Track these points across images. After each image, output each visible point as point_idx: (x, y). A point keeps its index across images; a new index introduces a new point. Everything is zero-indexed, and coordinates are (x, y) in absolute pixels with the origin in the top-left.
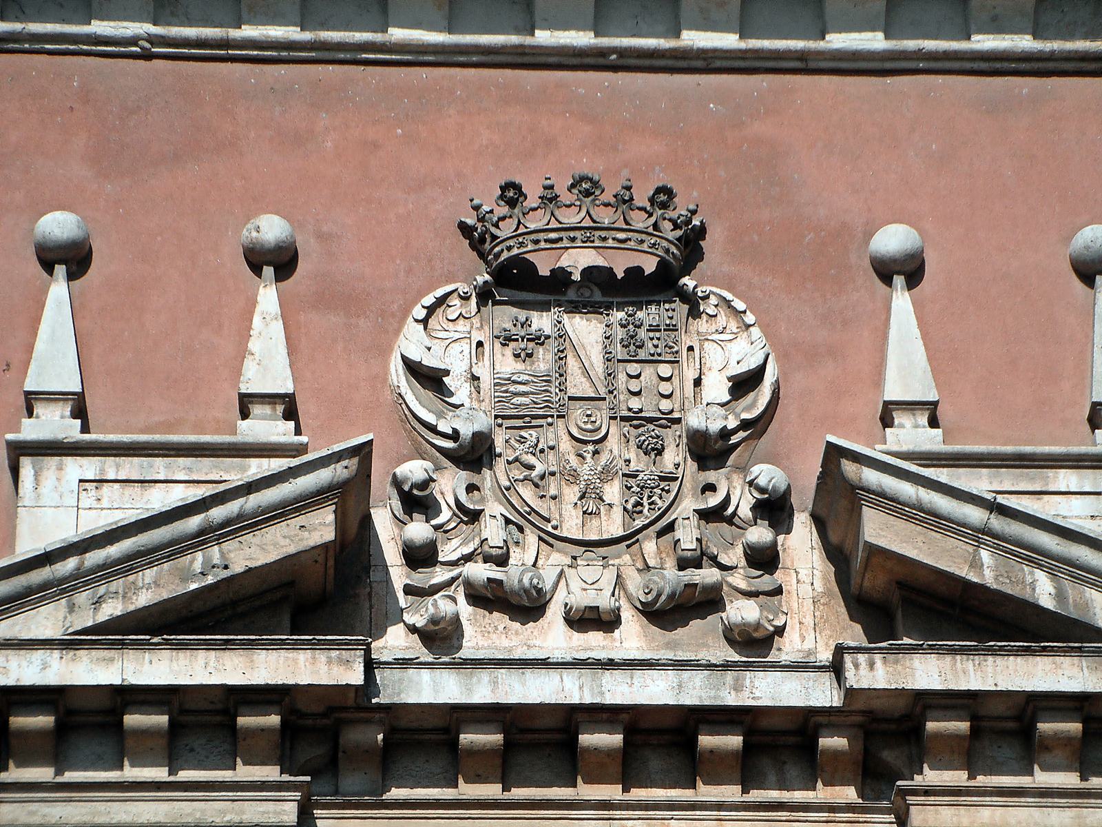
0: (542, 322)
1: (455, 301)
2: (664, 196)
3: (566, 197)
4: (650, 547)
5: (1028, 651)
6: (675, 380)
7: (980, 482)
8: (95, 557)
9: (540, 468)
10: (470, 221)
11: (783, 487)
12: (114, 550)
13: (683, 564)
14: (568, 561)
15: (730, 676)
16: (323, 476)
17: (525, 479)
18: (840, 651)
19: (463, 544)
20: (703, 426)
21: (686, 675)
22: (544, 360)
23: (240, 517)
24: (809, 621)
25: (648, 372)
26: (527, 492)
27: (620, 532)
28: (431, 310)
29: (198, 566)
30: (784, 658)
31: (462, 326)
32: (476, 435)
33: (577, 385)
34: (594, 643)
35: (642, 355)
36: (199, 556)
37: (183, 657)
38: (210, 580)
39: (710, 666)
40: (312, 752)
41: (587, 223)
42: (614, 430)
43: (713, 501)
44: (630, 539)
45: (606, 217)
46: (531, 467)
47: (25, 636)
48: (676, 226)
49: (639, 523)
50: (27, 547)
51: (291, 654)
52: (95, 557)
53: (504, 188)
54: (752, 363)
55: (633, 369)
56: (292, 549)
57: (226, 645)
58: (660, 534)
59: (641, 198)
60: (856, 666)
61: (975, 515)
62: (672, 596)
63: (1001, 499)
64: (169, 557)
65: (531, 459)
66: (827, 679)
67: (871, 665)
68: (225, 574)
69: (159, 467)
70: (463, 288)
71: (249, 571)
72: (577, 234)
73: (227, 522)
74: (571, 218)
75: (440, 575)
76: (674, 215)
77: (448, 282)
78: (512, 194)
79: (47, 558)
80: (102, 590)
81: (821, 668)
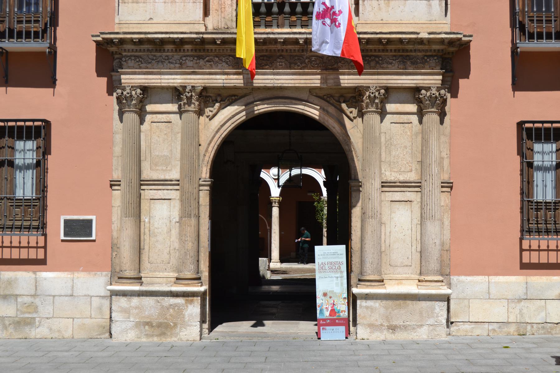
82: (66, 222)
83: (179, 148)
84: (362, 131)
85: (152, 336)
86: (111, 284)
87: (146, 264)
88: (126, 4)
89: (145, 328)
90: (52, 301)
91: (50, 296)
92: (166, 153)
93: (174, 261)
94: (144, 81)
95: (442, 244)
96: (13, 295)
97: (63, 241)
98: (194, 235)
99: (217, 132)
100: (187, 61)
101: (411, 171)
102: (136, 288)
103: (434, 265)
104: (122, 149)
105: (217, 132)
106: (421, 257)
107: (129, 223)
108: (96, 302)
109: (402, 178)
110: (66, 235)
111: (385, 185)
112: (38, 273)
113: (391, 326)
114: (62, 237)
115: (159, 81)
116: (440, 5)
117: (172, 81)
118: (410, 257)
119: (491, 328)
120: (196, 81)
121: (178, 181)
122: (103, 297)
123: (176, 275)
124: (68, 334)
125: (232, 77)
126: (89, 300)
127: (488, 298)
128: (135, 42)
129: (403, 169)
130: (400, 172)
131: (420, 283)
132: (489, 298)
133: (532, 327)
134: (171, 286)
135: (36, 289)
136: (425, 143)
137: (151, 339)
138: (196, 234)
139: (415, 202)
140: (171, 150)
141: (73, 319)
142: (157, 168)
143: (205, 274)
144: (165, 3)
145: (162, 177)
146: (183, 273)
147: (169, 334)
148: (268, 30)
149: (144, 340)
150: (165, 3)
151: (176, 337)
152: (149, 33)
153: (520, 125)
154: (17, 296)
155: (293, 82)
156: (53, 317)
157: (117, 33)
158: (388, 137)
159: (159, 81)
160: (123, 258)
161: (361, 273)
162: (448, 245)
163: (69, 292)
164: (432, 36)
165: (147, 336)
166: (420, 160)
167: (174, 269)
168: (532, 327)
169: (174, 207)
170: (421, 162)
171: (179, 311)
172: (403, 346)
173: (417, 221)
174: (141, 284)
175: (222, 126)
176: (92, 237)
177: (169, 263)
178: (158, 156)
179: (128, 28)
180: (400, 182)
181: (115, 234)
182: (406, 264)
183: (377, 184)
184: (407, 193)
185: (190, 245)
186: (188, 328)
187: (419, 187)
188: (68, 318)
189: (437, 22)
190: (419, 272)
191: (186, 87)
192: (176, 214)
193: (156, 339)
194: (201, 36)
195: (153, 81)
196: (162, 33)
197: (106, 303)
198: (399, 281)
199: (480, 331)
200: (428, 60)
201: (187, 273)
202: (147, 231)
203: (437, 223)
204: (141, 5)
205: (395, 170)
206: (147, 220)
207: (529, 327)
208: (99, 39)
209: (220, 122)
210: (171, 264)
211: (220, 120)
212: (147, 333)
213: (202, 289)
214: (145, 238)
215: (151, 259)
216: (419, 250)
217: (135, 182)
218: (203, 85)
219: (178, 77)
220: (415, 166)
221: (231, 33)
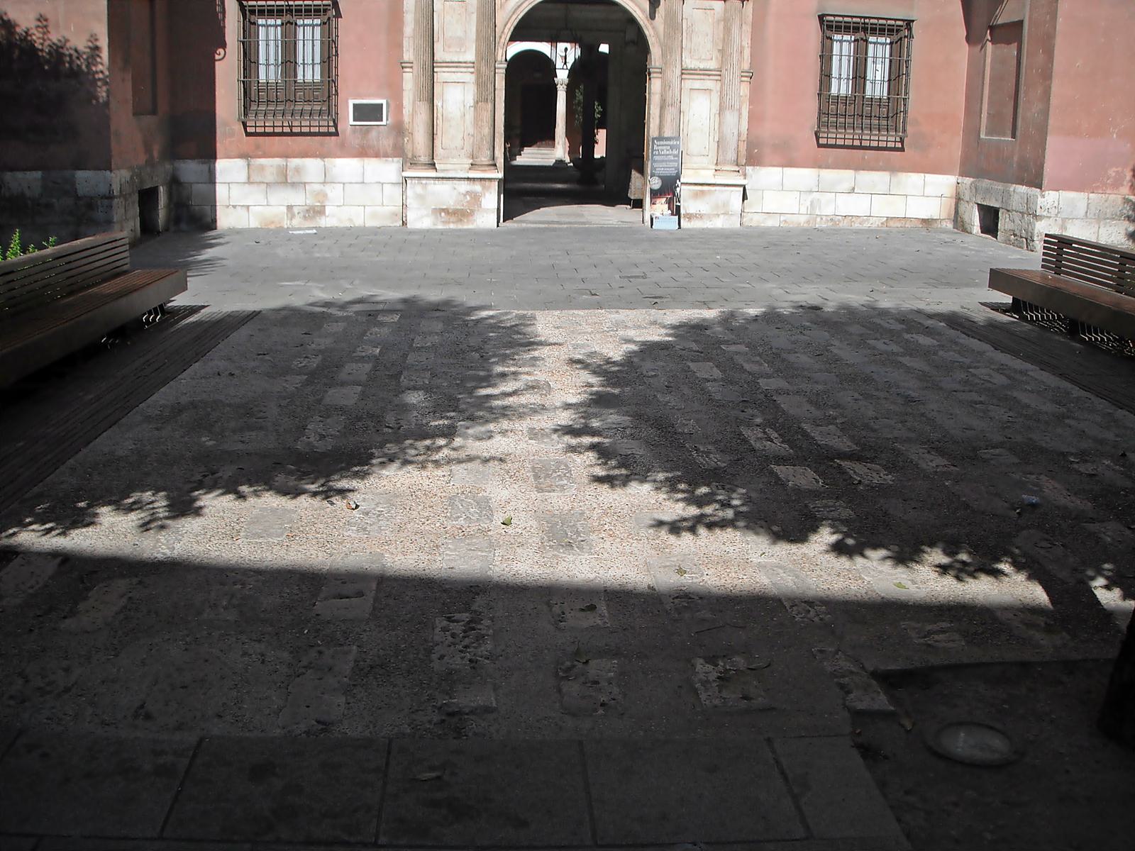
82: (355, 106)
83: (474, 29)
84: (663, 16)
85: (449, 222)
87: (439, 151)
89: (440, 214)
92: (460, 33)
93: (468, 148)
95: (739, 135)
96: (302, 183)
98: (491, 122)
99: (514, 13)
103: (731, 155)
104: (414, 30)
105: (514, 13)
106: (718, 146)
107: (423, 109)
111: (684, 71)
113: (688, 214)
114: (352, 122)
118: (707, 147)
119: (782, 218)
121: (474, 63)
123: (471, 161)
129: (703, 57)
130: (700, 59)
133: (822, 219)
134: (468, 172)
136: (727, 30)
138: (493, 118)
141: (364, 206)
142: (451, 50)
146: (479, 160)
147: (465, 221)
149: (440, 226)
151: (473, 224)
154: (305, 183)
158: (689, 24)
160: (417, 144)
162: (746, 136)
163: (360, 180)
166: (721, 48)
167: (469, 155)
168: (822, 219)
170: (722, 52)
171: (476, 198)
173: (715, 110)
175: (519, 7)
177: (463, 149)
180: (701, 70)
181: (406, 119)
183: (678, 72)
184: (708, 81)
185: (487, 130)
192: (470, 100)
197: (398, 190)
199: (771, 223)
201: (483, 159)
203: (736, 114)
205: (695, 57)
206: (440, 105)
207: (818, 219)
210: (465, 149)
212: (443, 220)
214: (439, 122)
216: (717, 139)
217: (429, 63)
220: (715, 54)
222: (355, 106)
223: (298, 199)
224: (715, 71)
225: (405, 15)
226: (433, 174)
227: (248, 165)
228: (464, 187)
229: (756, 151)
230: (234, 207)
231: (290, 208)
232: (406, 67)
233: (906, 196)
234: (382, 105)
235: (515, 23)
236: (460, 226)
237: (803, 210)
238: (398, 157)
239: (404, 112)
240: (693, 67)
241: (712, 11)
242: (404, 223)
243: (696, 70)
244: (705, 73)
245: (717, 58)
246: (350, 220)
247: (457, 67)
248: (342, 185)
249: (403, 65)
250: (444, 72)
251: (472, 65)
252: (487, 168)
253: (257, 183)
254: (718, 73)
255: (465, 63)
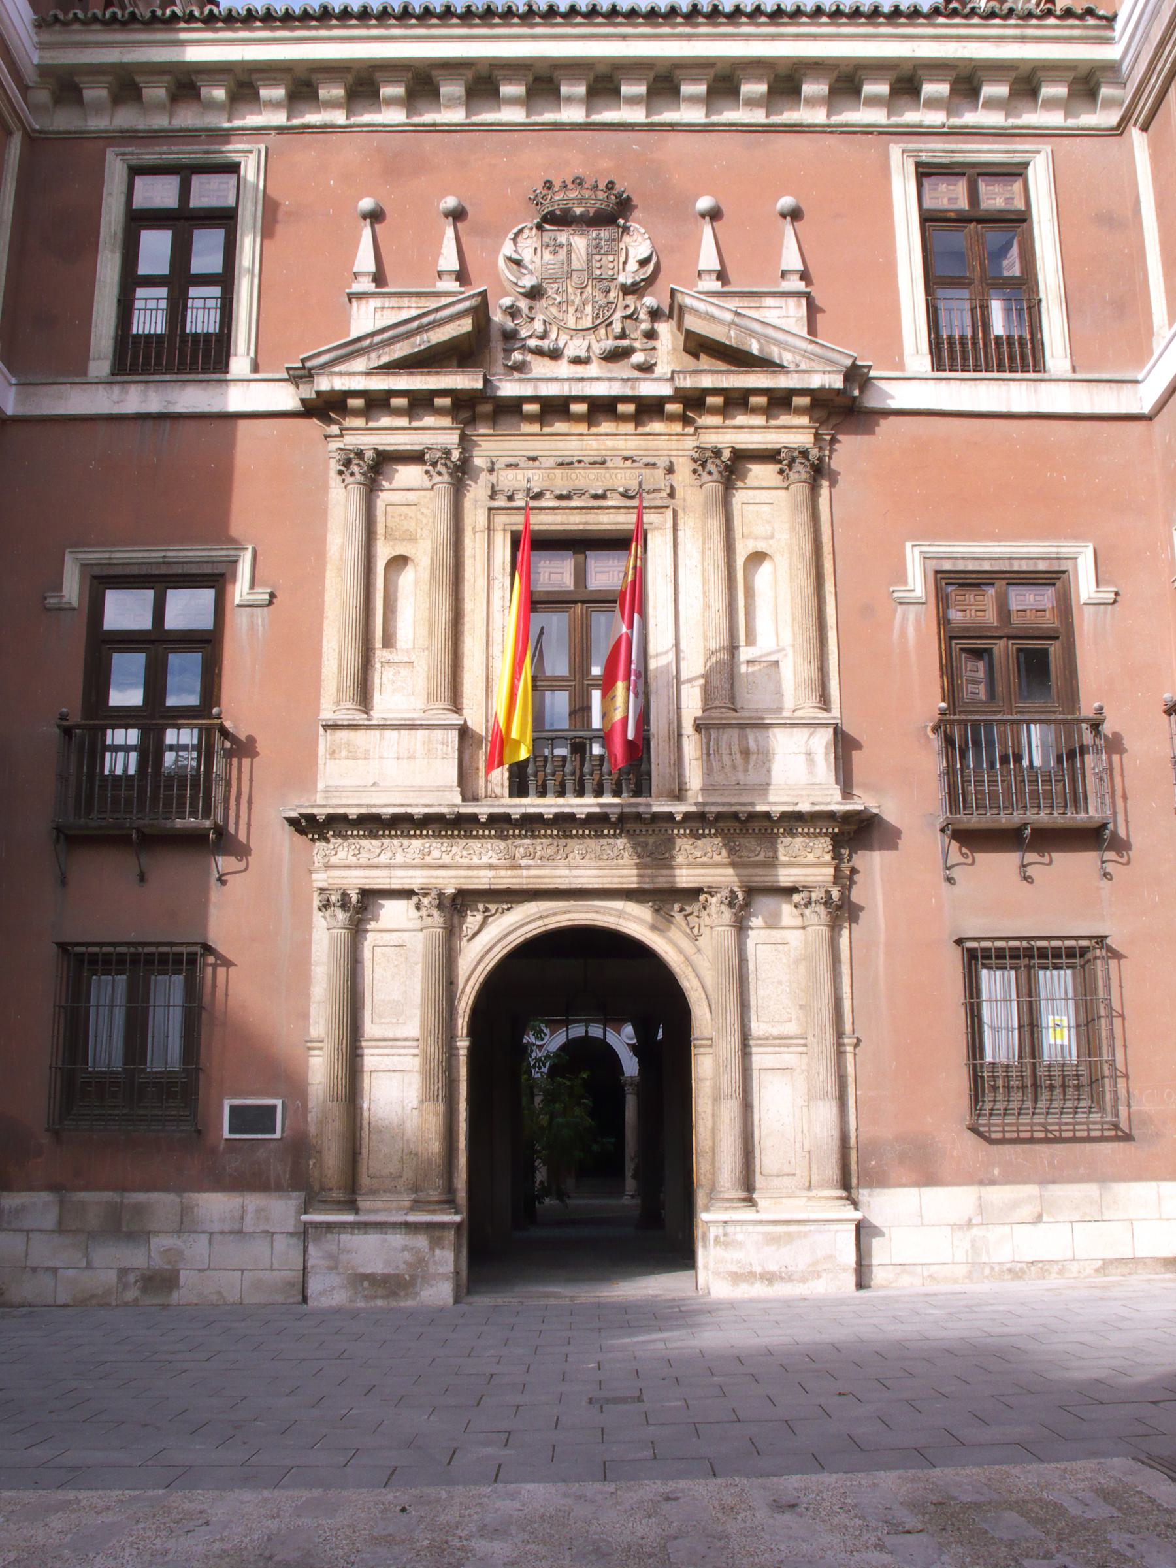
0: (562, 238)
1: (526, 231)
2: (611, 186)
3: (570, 186)
4: (602, 331)
5: (747, 372)
6: (616, 263)
7: (733, 304)
8: (377, 339)
9: (559, 299)
10: (532, 197)
11: (655, 307)
12: (385, 336)
13: (616, 338)
14: (569, 337)
15: (630, 383)
16: (467, 304)
17: (553, 304)
18: (673, 372)
19: (528, 331)
20: (624, 282)
21: (612, 383)
22: (562, 254)
23: (434, 321)
24: (665, 360)
25: (604, 258)
26: (554, 310)
27: (590, 326)
28: (517, 235)
29: (418, 342)
30: (655, 376)
31: (529, 241)
32: (533, 287)
33: (575, 265)
34: (580, 371)
35: (602, 252)
36: (419, 338)
37: (412, 378)
38: (423, 347)
39: (622, 379)
40: (465, 415)
41: (579, 197)
42: (590, 283)
43: (629, 312)
44: (594, 328)
45: (587, 194)
46: (555, 299)
47: (351, 370)
48: (616, 198)
49: (598, 322)
50: (354, 334)
51: (454, 377)
52: (377, 339)
53: (545, 183)
54: (646, 255)
55: (598, 258)
56: (455, 334)
57: (429, 373)
58: (607, 326)
59: (602, 186)
60: (679, 379)
61: (728, 317)
62: (610, 351)
63: (739, 311)
64: (407, 338)
65: (555, 296)
66: (668, 384)
67: (685, 378)
68: (428, 345)
69: (405, 302)
70: (530, 225)
71: (438, 344)
72: (575, 201)
73: (429, 324)
74: (573, 195)
75: (518, 345)
76: (615, 193)
77: (523, 222)
78: (548, 185)
79: (359, 339)
80: (381, 352)
81: (667, 380)
82: (233, 1109)
85: (375, 1297)
86: (306, 1213)
87: (365, 1181)
88: (337, 761)
90: (207, 1242)
91: (203, 1232)
94: (364, 881)
97: (226, 1140)
100: (432, 848)
101: (790, 1021)
102: (349, 1218)
108: (281, 1243)
109: (775, 1031)
110: (231, 1131)
112: (186, 1195)
114: (226, 1134)
115: (388, 880)
116: (827, 760)
117: (408, 881)
120: (446, 881)
121: (418, 1040)
122: (291, 1234)
123: (413, 1196)
124: (232, 1297)
125: (503, 873)
126: (269, 1239)
127: (919, 1223)
128: (352, 820)
129: (777, 1018)
131: (811, 1203)
132: (922, 1225)
133: (992, 1269)
134: (406, 1214)
135: (182, 1222)
137: (372, 1304)
139: (799, 1071)
140: (405, 992)
141: (243, 1271)
142: (383, 1020)
143: (462, 1195)
144: (398, 759)
145: (391, 1035)
148: (561, 801)
149: (361, 1304)
150: (398, 759)
151: (414, 1299)
152: (375, 806)
153: (959, 942)
154: (149, 1232)
155: (600, 880)
156: (209, 1268)
157: (324, 806)
159: (388, 880)
161: (713, 1189)
163: (236, 1227)
164: (817, 808)
165: (367, 1298)
168: (992, 1269)
169: (410, 1084)
172: (787, 1303)
174: (357, 1211)
176: (275, 1133)
178: (383, 1001)
179: (340, 797)
180: (775, 1038)
182: (787, 1170)
186: (433, 1282)
187: (805, 1045)
188: (234, 1270)
189: (824, 787)
190: (807, 1184)
191: (430, 889)
193: (380, 1303)
194: (456, 810)
195: (379, 881)
196: (395, 805)
198: (776, 1200)
200: (811, 844)
202: (365, 1123)
204: (360, 762)
208: (294, 814)
209: (485, 946)
210: (404, 1178)
211: (484, 943)
212: (366, 1293)
213: (457, 1218)
215: (371, 1170)
218: (458, 886)
219: (418, 873)
221: (503, 805)
222: (233, 1109)
223: (136, 1258)
224: (797, 1038)
225: (313, 967)
226: (349, 1218)
227: (62, 1203)
228: (398, 1239)
229: (873, 1163)
230: (34, 1270)
231: (123, 1272)
232: (314, 1049)
233: (1131, 1221)
234: (274, 1107)
235: (481, 979)
236: (394, 1304)
237: (960, 1256)
238: (300, 1191)
239: (309, 1120)
240: (761, 1033)
241: (786, 947)
242: (305, 1300)
243: (767, 1039)
244: (782, 1041)
245: (798, 1018)
246: (220, 1293)
247: (392, 1047)
248: (207, 1236)
249: (309, 1045)
250: (372, 1055)
251: (415, 1043)
252: (437, 1207)
253: (71, 1230)
254: (802, 1041)
255: (406, 1040)
